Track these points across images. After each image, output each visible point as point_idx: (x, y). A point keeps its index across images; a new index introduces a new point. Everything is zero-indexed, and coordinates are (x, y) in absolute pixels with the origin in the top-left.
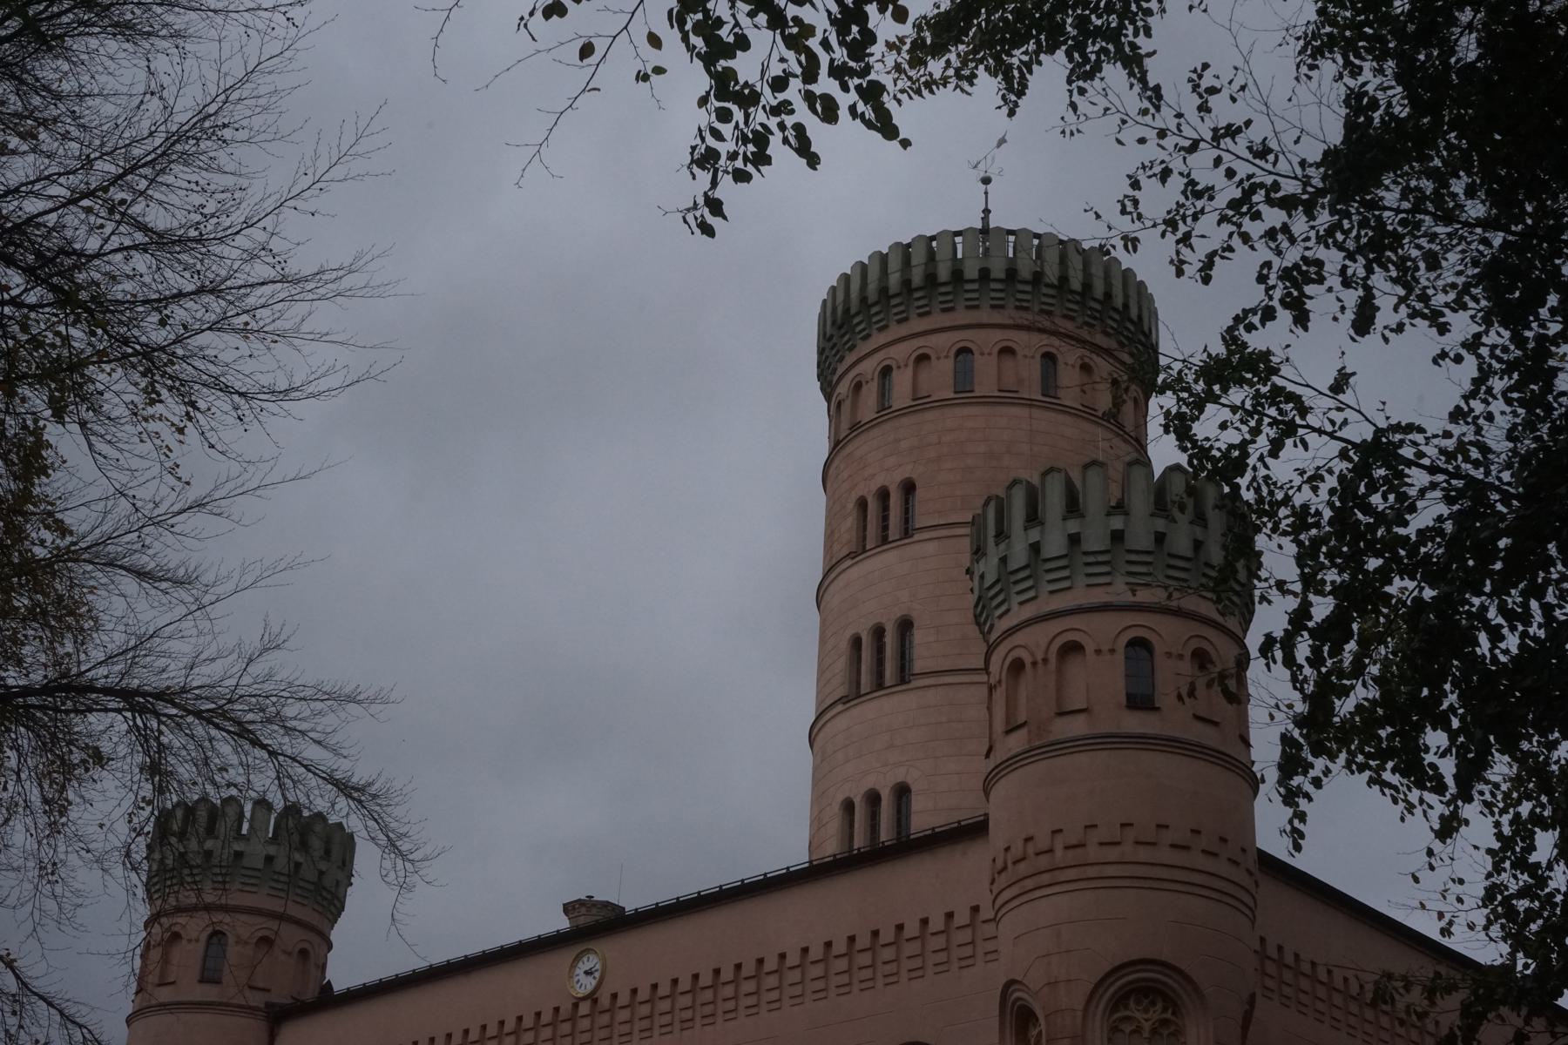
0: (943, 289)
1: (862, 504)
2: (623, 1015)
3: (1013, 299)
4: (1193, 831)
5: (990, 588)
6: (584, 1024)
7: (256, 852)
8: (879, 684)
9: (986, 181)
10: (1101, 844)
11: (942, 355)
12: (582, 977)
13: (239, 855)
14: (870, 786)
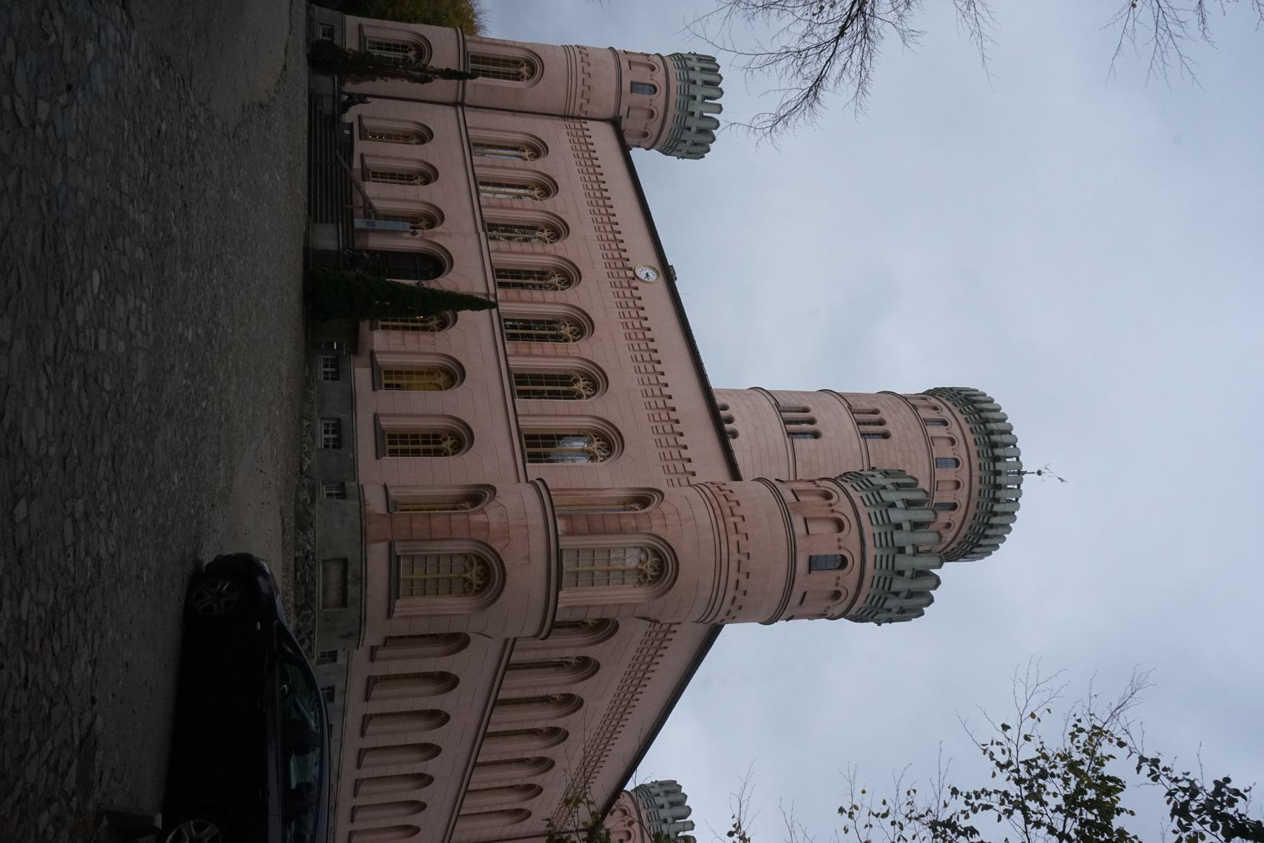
0: (990, 452)
1: (876, 412)
2: (628, 294)
3: (984, 487)
4: (746, 591)
5: (867, 480)
6: (622, 274)
7: (696, 107)
8: (787, 422)
9: (1039, 473)
10: (738, 542)
11: (954, 451)
12: (646, 272)
13: (694, 98)
14: (736, 418)
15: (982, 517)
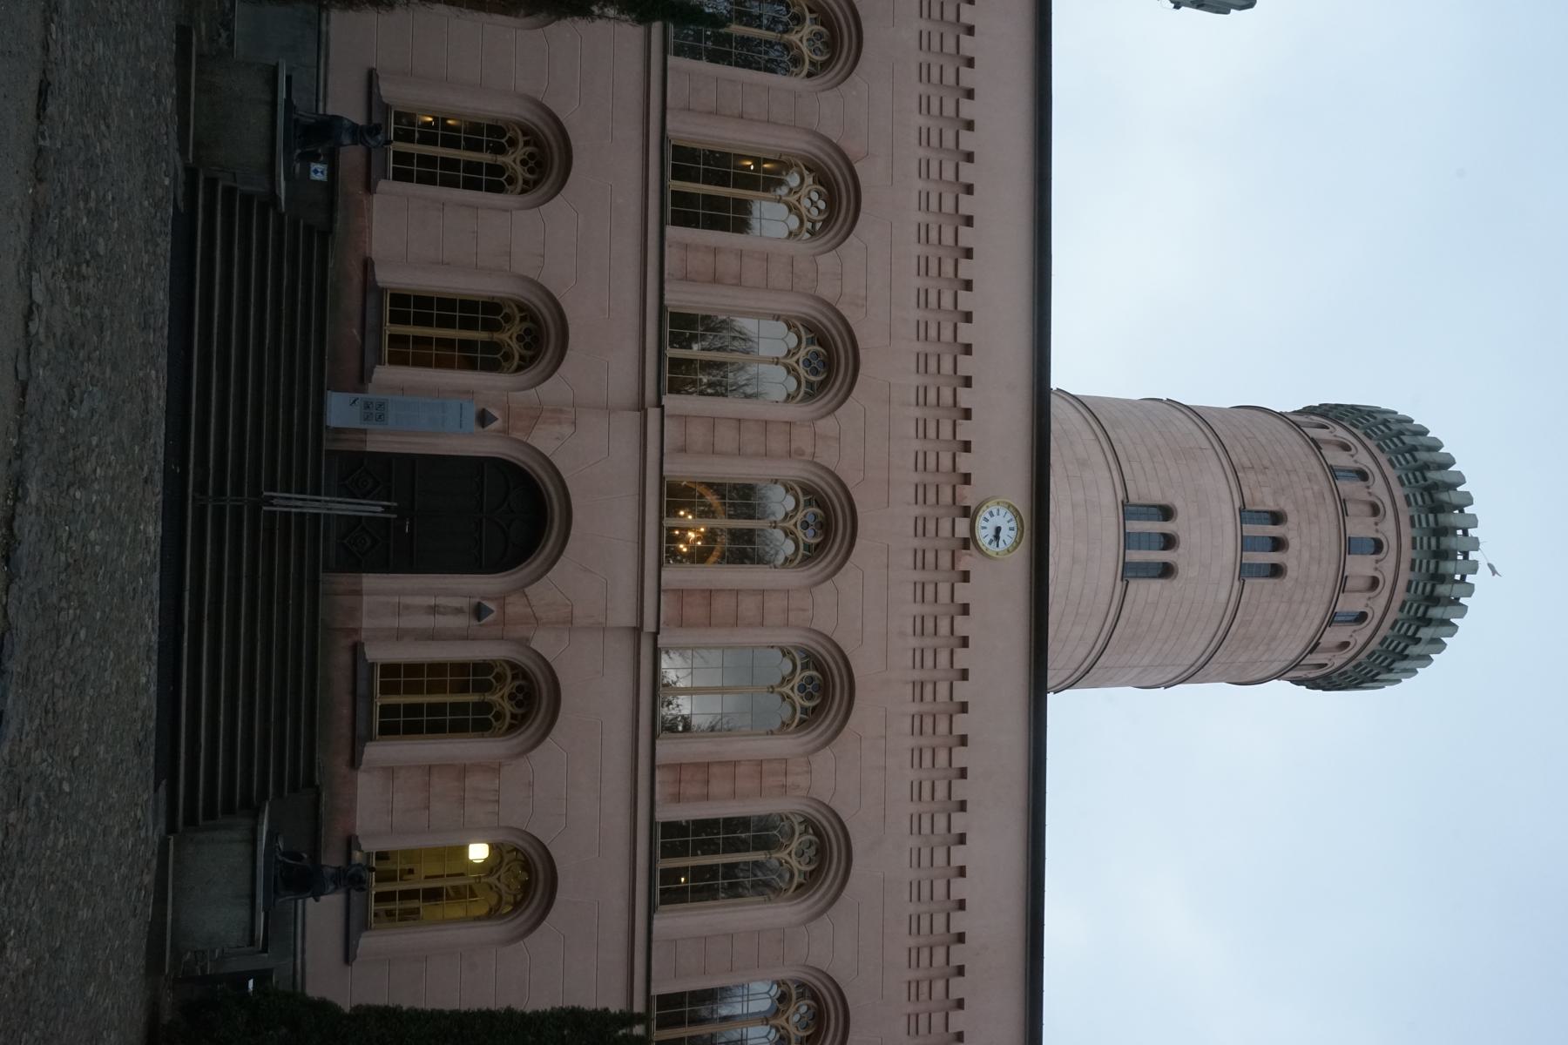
15: (1406, 626)
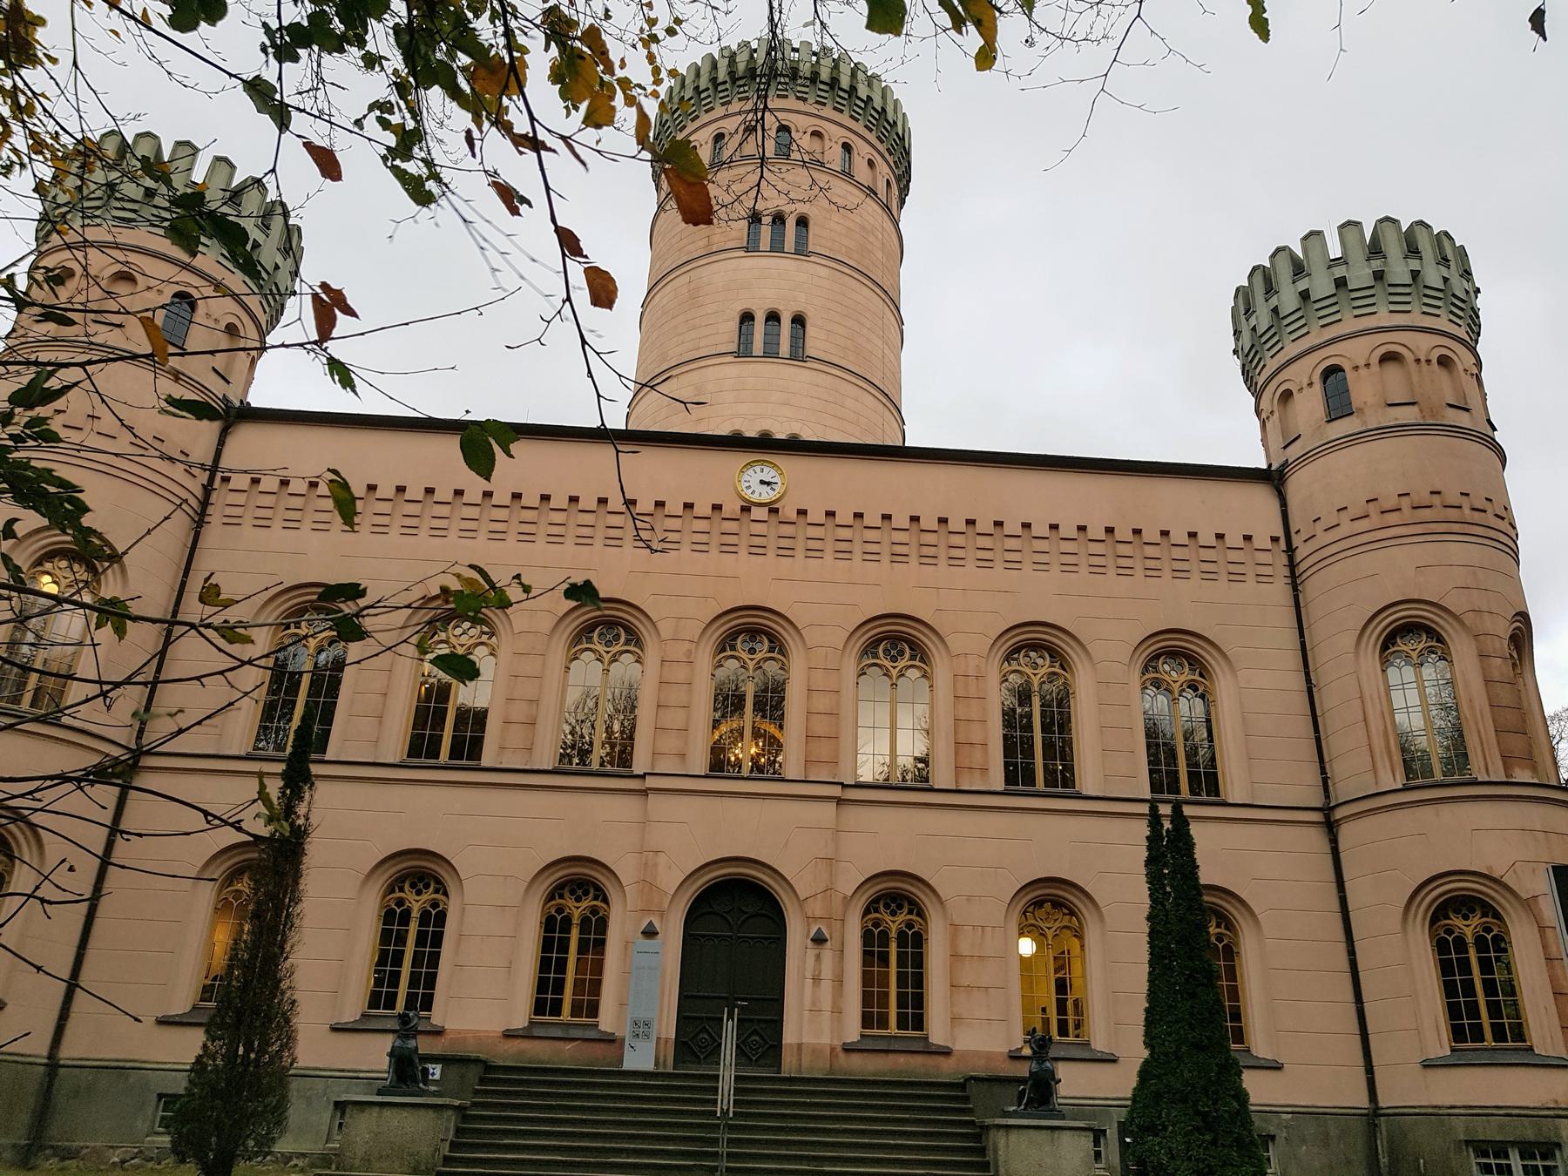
5: (1261, 336)
